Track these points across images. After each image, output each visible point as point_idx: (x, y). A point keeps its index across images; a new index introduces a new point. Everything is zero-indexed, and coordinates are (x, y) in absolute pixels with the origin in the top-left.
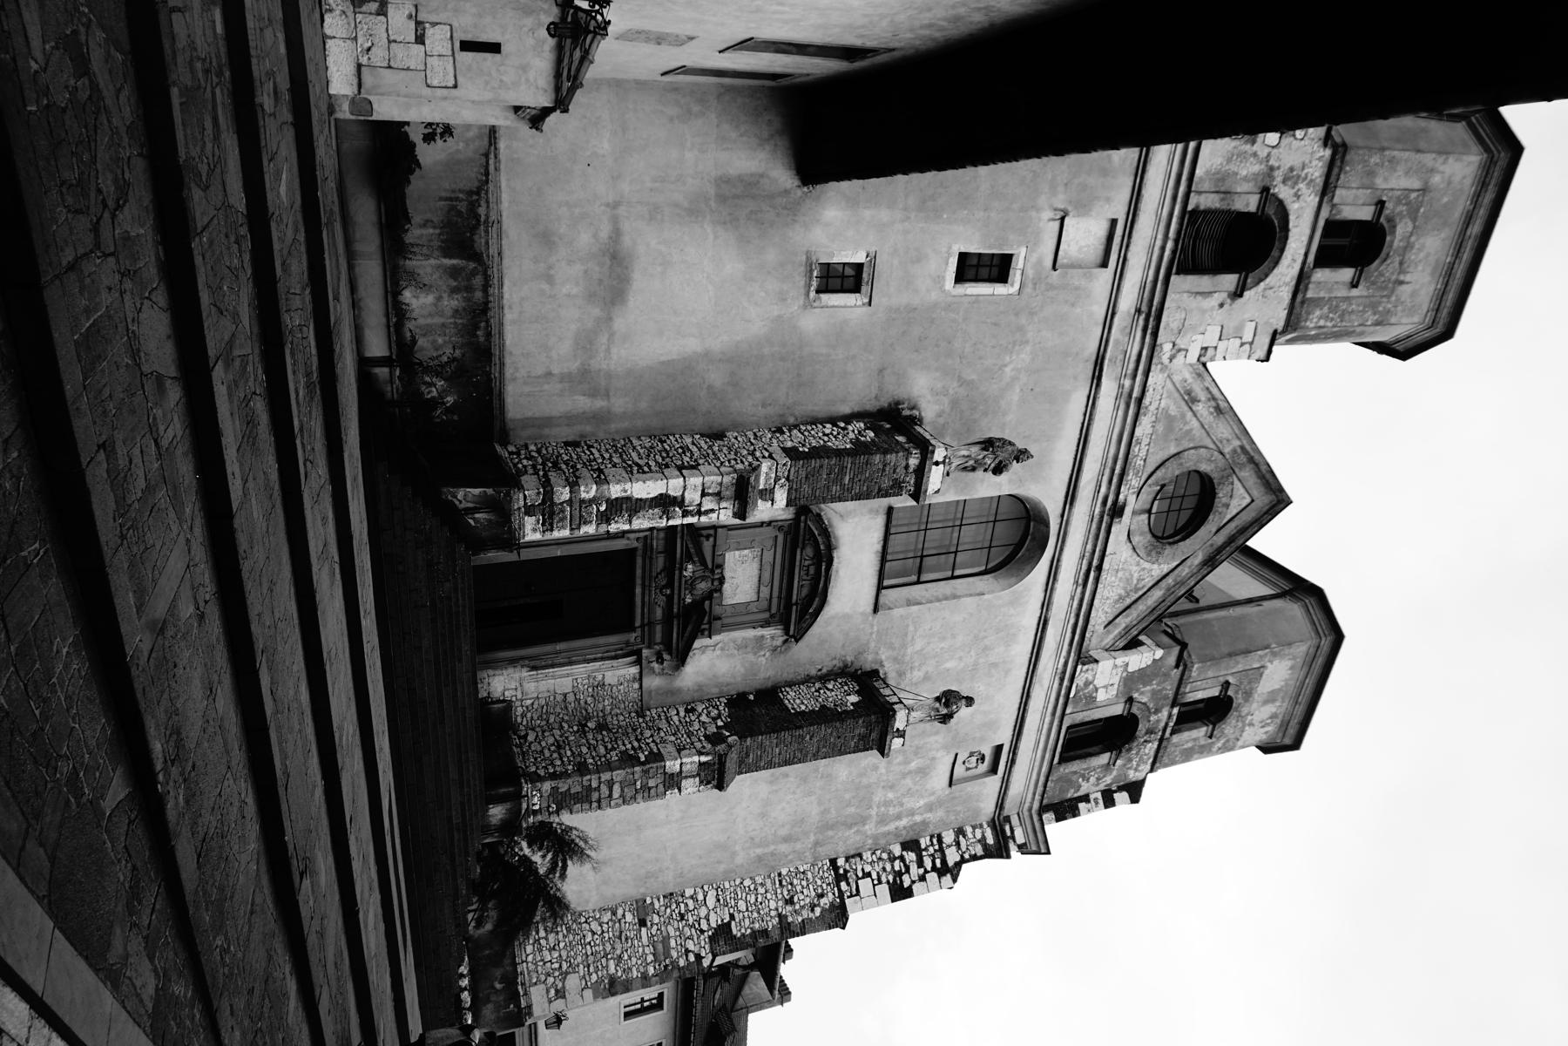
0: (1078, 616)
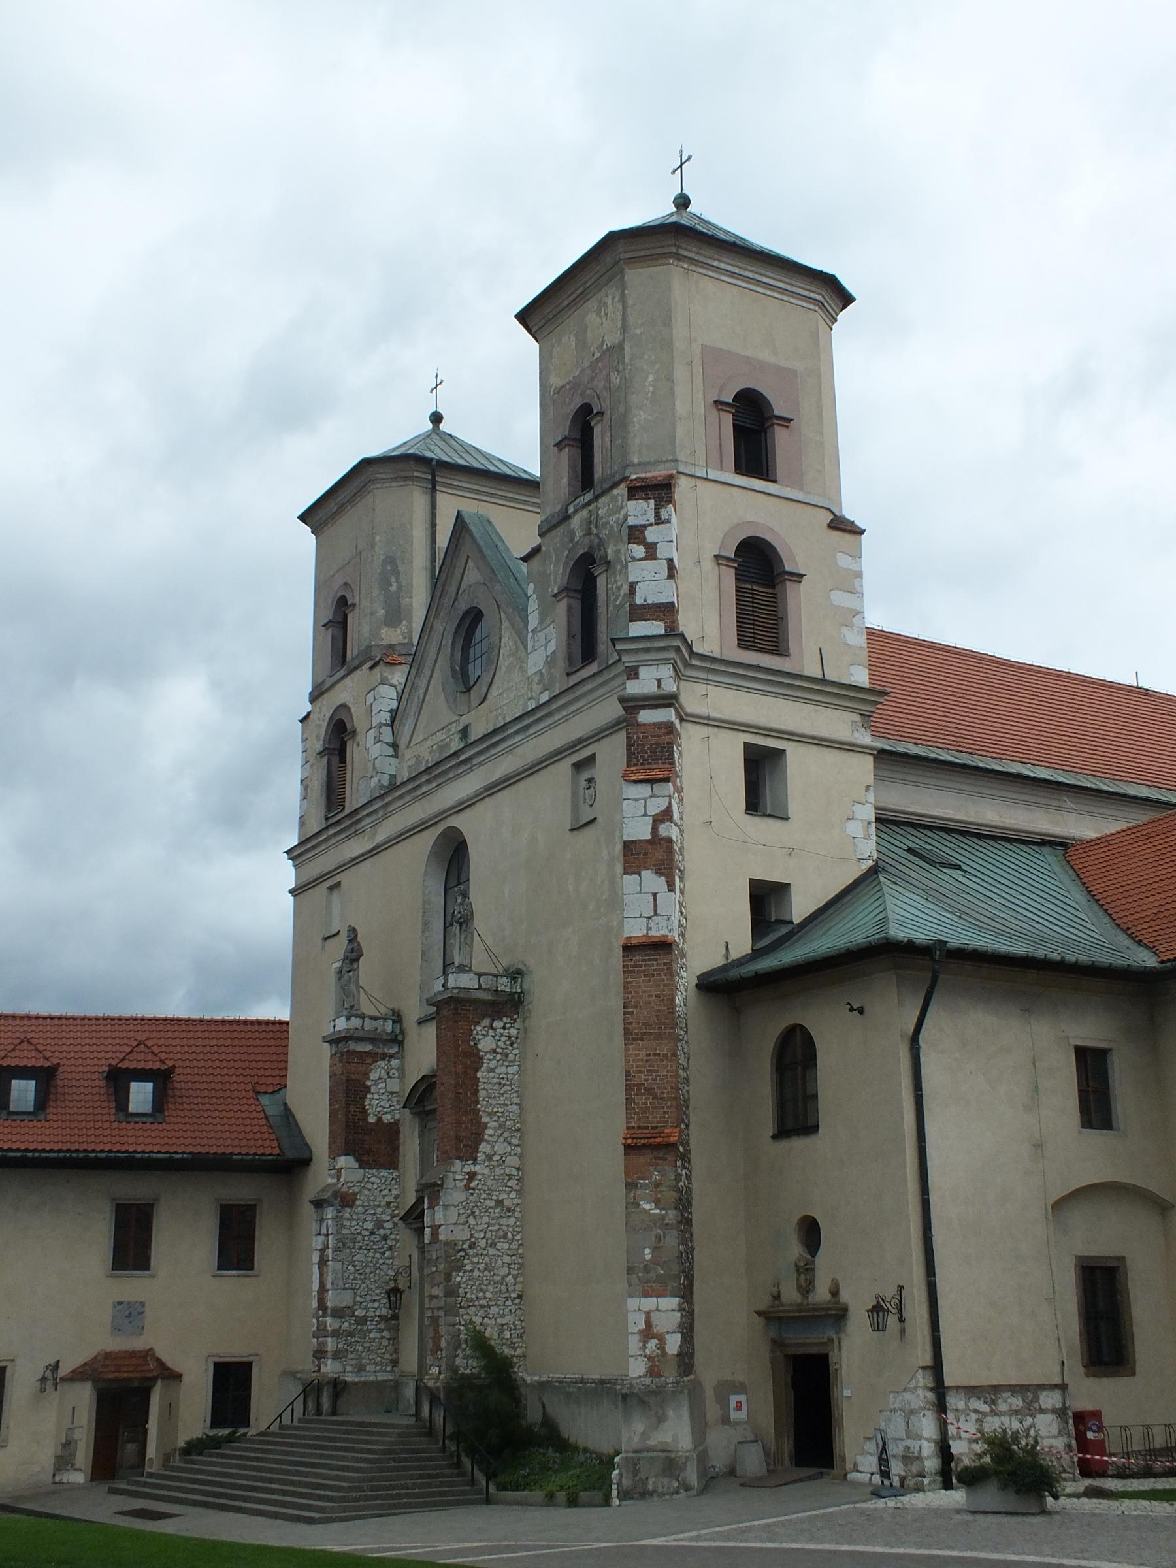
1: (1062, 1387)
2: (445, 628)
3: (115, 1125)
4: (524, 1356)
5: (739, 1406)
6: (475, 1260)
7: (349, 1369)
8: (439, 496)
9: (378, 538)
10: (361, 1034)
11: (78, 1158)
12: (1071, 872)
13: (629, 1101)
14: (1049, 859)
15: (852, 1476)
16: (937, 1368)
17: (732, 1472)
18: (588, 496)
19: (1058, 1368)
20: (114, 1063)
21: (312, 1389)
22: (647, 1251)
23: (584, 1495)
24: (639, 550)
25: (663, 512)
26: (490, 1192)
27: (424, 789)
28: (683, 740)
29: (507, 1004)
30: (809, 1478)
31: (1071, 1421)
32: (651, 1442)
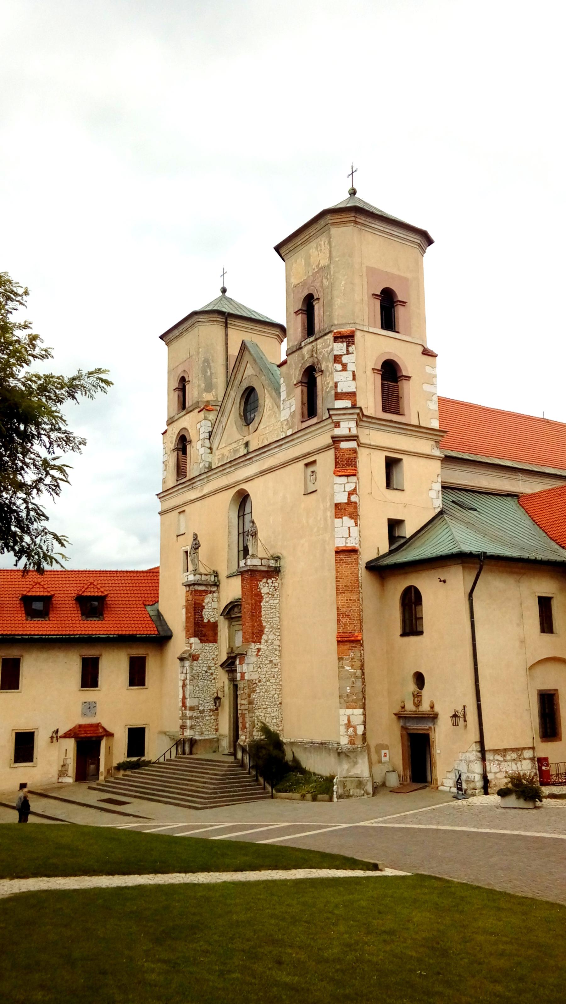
0: (261, 454)
1: (533, 748)
2: (236, 395)
3: (81, 622)
4: (282, 730)
5: (385, 756)
6: (261, 687)
7: (197, 733)
8: (229, 330)
9: (200, 350)
10: (200, 582)
11: (65, 638)
12: (523, 510)
13: (339, 621)
14: (511, 504)
15: (441, 788)
16: (481, 742)
17: (384, 784)
18: (312, 339)
19: (531, 740)
20: (80, 593)
21: (179, 743)
22: (348, 688)
23: (319, 796)
24: (339, 367)
25: (350, 349)
26: (267, 657)
27: (228, 470)
28: (359, 455)
29: (274, 572)
30: (421, 788)
31: (536, 763)
32: (351, 774)
